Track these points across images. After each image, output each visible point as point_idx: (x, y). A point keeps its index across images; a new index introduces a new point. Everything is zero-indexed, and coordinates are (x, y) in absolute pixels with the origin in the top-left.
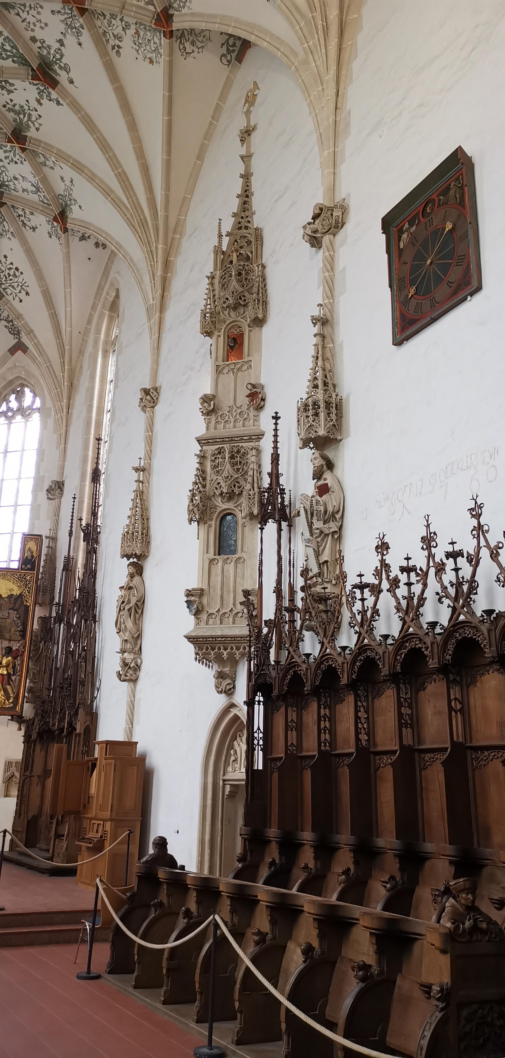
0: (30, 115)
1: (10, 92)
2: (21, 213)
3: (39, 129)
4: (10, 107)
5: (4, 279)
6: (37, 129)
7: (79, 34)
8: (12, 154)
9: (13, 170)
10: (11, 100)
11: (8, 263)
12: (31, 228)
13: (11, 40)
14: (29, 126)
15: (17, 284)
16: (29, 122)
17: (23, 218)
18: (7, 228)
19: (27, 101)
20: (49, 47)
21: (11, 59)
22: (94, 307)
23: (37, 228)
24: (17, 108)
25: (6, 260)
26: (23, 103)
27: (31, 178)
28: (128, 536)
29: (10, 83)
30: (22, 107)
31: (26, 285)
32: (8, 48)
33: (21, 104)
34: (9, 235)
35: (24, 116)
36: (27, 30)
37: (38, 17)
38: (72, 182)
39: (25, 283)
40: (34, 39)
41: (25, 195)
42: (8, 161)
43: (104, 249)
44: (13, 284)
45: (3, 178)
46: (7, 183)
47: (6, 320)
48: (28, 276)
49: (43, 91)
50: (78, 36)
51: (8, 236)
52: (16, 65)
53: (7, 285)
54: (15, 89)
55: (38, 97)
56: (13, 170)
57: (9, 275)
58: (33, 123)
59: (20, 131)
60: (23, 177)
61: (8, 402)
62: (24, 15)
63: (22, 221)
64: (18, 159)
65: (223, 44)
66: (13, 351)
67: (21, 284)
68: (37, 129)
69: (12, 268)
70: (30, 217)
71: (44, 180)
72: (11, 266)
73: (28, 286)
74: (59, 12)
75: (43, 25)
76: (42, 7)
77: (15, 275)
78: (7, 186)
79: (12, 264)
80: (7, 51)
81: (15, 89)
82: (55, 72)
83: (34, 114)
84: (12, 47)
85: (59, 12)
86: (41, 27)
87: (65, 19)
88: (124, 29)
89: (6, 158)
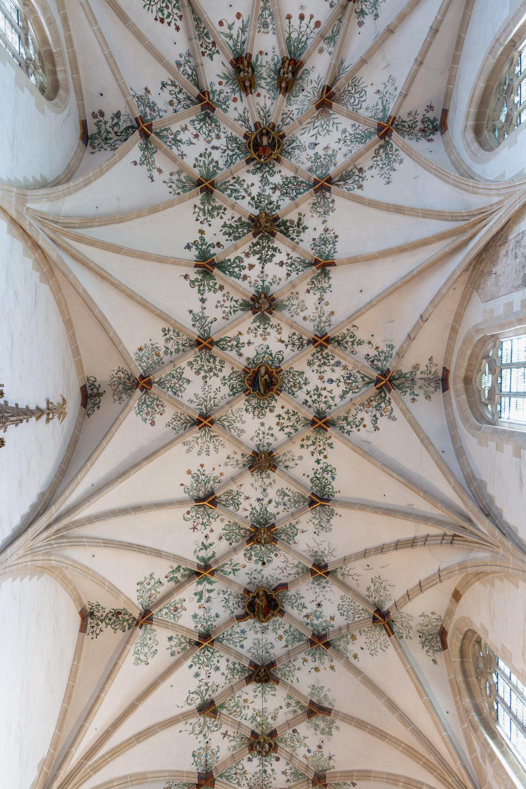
0: (204, 214)
1: (225, 225)
2: (181, 96)
3: (194, 208)
4: (221, 211)
6: (195, 206)
7: (194, 319)
8: (207, 162)
9: (201, 145)
10: (221, 218)
11: (172, 24)
13: (236, 277)
14: (202, 203)
16: (203, 207)
17: (177, 90)
18: (187, 68)
19: (210, 225)
20: (210, 290)
21: (232, 261)
22: (69, 40)
23: (161, 89)
24: (215, 213)
25: (175, 24)
26: (213, 221)
27: (184, 148)
29: (227, 234)
30: (212, 216)
32: (236, 270)
33: (213, 219)
34: (182, 60)
36: (228, 293)
37: (224, 309)
38: (152, 178)
39: (149, 8)
40: (221, 288)
41: (183, 123)
42: (208, 152)
43: (94, 113)
45: (206, 127)
46: (202, 124)
49: (202, 245)
50: (194, 317)
51: (183, 59)
52: (227, 258)
54: (221, 230)
55: (204, 236)
56: (201, 145)
57: (167, 7)
58: (200, 209)
59: (207, 193)
60: (191, 143)
62: (233, 303)
63: (176, 87)
65: (99, 386)
68: (195, 206)
69: (167, 18)
70: (170, 98)
71: (174, 159)
72: (169, 20)
73: (145, 6)
74: (212, 323)
75: (219, 305)
76: (224, 318)
77: (161, 10)
78: (201, 121)
79: (169, 24)
80: (236, 267)
81: (221, 230)
82: (198, 273)
84: (233, 272)
85: (212, 323)
86: (219, 302)
87: (206, 321)
88: (167, 348)
89: (210, 153)
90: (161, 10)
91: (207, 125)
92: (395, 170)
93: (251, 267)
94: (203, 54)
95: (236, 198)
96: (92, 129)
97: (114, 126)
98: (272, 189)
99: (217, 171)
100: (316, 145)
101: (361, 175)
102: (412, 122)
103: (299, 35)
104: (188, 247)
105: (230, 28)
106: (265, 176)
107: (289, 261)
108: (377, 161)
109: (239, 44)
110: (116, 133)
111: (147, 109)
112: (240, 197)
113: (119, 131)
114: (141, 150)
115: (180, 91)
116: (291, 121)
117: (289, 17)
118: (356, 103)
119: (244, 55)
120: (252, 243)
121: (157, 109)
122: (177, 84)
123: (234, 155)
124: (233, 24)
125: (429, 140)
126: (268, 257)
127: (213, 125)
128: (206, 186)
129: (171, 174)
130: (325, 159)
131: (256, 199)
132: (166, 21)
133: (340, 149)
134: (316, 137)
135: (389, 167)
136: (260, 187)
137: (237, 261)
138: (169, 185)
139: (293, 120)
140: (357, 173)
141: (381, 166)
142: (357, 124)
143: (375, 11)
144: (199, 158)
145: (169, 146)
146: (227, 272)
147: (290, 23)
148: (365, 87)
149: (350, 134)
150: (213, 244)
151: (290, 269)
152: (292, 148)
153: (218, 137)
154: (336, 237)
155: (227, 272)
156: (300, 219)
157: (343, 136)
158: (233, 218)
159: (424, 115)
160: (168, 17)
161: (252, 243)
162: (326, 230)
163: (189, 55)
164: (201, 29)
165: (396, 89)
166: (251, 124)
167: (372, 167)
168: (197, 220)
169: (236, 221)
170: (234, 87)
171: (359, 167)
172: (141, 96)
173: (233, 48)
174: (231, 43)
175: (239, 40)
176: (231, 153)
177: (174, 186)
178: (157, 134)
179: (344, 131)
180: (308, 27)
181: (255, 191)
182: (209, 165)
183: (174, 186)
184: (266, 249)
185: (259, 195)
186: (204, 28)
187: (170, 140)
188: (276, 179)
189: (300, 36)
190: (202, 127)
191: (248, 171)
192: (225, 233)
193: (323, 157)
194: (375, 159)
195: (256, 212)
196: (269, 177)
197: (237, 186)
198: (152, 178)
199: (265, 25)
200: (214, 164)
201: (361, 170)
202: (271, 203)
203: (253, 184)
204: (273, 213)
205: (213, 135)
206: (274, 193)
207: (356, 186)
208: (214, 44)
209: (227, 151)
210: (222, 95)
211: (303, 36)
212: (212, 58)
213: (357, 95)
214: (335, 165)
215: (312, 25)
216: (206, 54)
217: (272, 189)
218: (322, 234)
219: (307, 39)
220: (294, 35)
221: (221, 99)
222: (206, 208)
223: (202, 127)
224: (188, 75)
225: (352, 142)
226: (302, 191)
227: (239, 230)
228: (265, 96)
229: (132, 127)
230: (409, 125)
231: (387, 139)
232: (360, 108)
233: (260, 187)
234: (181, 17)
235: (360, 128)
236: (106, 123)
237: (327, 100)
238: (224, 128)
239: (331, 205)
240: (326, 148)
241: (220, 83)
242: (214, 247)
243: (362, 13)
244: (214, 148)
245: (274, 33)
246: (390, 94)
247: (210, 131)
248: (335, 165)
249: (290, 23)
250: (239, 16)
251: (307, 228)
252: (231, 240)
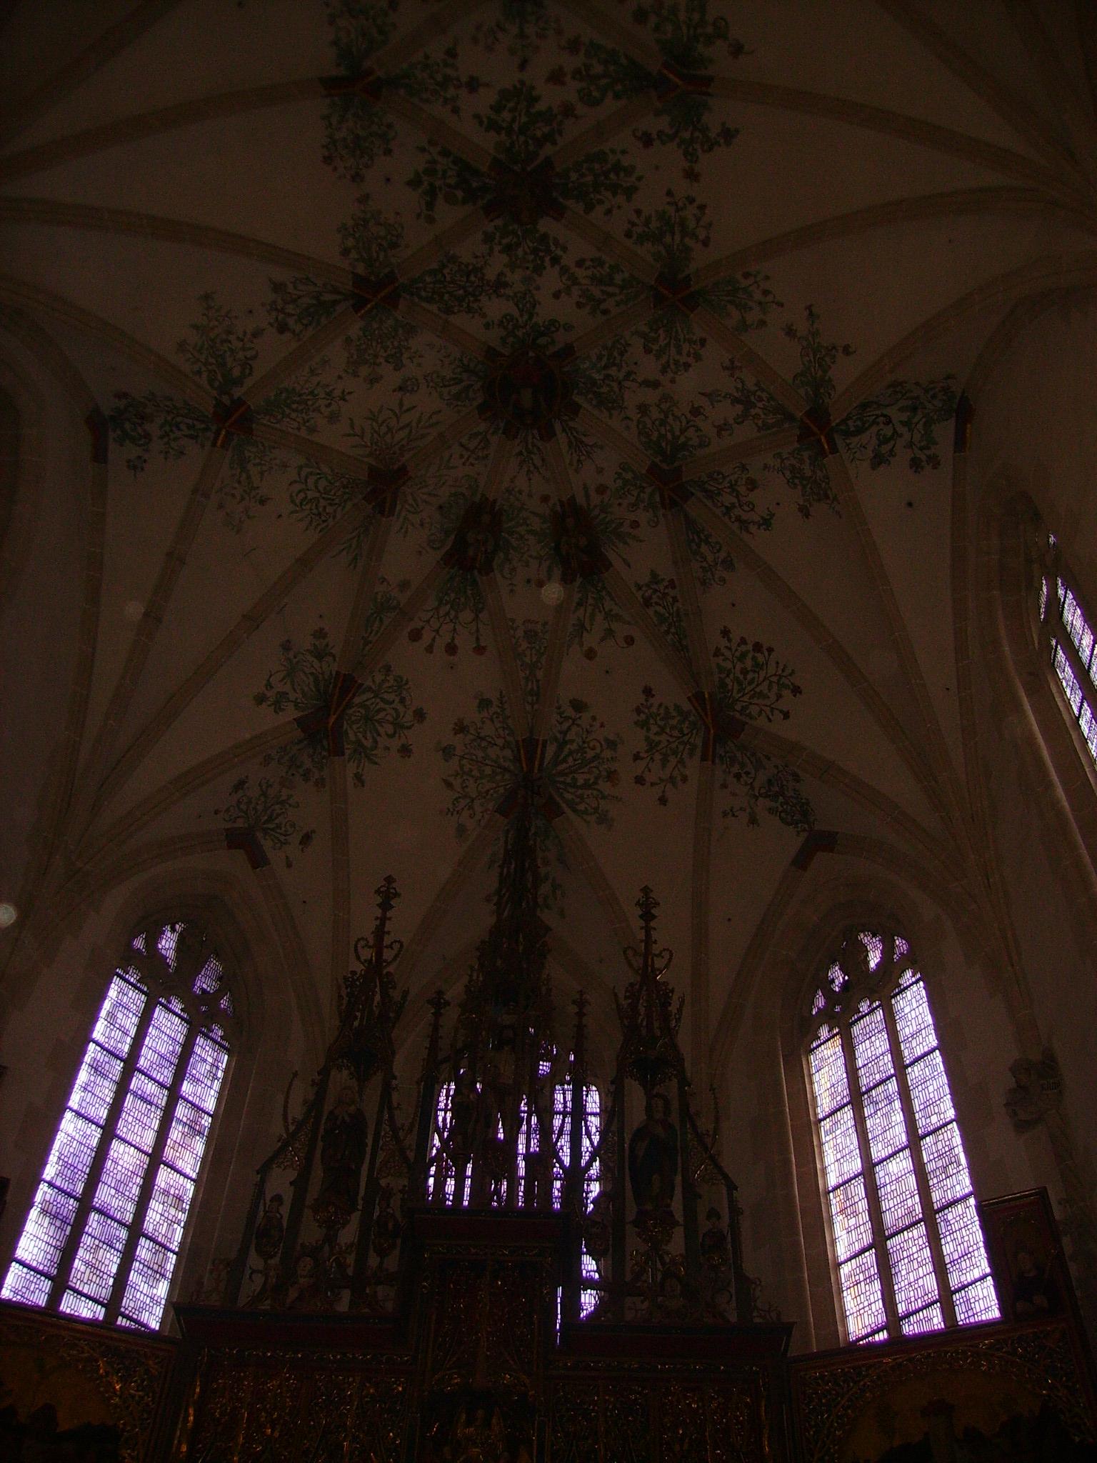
1: (630, 192)
2: (728, 499)
3: (708, 238)
4: (639, 230)
5: (736, 687)
6: (706, 243)
8: (673, 350)
12: (760, 526)
15: (766, 683)
16: (687, 240)
17: (737, 511)
18: (710, 558)
19: (669, 193)
21: (610, 95)
24: (654, 224)
25: (729, 640)
31: (788, 671)
32: (598, 69)
35: (673, 234)
38: (811, 314)
42: (670, 375)
44: (758, 690)
46: (682, 439)
47: (767, 796)
53: (746, 698)
54: (639, 179)
57: (744, 672)
63: (738, 519)
64: (688, 355)
66: (802, 861)
67: (774, 679)
69: (748, 652)
72: (744, 648)
77: (758, 666)
79: (743, 641)
89: (664, 371)
90: (758, 666)
91: (669, 436)
92: (195, 327)
93: (556, 77)
94: (672, 584)
95: (599, 262)
96: (945, 432)
97: (892, 438)
98: (506, 285)
99: (646, 330)
100: (400, 388)
101: (281, 317)
102: (172, 436)
103: (456, 617)
104: (728, 135)
105: (610, 633)
106: (526, 317)
107: (451, 92)
108: (243, 349)
109: (590, 601)
110: (889, 421)
111: (808, 473)
112: (588, 263)
113: (882, 426)
114: (830, 380)
115: (728, 509)
116: (464, 441)
117: (480, 650)
118: (311, 481)
119: (579, 580)
120: (554, 143)
121: (788, 474)
122: (735, 526)
123: (606, 367)
124: (602, 640)
125: (125, 395)
126: (511, 105)
127: (655, 436)
128: (676, 294)
129: (763, 323)
130: (376, 356)
131: (547, 259)
132: (750, 647)
133: (340, 377)
134: (401, 405)
135: (212, 335)
136: (538, 288)
137: (595, 94)
138: (770, 298)
139: (462, 445)
140: (291, 322)
141: (232, 337)
142: (303, 433)
143: (291, 655)
144: (691, 360)
145: (763, 390)
146: (624, 61)
147: (478, 639)
148: (296, 512)
149: (318, 410)
150: (663, 143)
151: (449, 71)
152: (461, 381)
153: (643, 409)
154: (328, 160)
155: (624, 61)
156: (430, 205)
157: (334, 407)
158: (609, 212)
159: (147, 451)
160: (743, 656)
161: (554, 143)
162: (357, 177)
163: (703, 583)
164: (673, 630)
165: (221, 506)
166: (562, 437)
167: (255, 335)
168: (702, 208)
169: (601, 202)
170: (603, 516)
171: (288, 335)
172: (819, 500)
173: (604, 593)
174: (608, 605)
175: (590, 609)
176: (613, 371)
177: (758, 296)
178: (791, 418)
179: (333, 418)
180: (437, 631)
181: (551, 279)
182: (669, 344)
183: (758, 296)
184: (516, 127)
185: (539, 270)
186: (667, 632)
187: (760, 405)
188: (496, 308)
189: (453, 613)
190: (682, 432)
191: (568, 328)
192: (629, 171)
193: (382, 360)
194: (249, 354)
195: (546, 225)
196: (516, 313)
197: (596, 292)
198: (811, 314)
200: (655, 347)
201: (283, 328)
202: (508, 249)
203: (556, 295)
204: (499, 222)
205: (655, 414)
206: (501, 274)
207: (290, 288)
208: (647, 602)
209: (621, 375)
210: (632, 499)
211: (448, 614)
212: (654, 575)
213: (310, 495)
214: (348, 341)
215: (427, 637)
216: (666, 583)
217: (506, 285)
218: (367, 166)
219: (437, 609)
220: (467, 615)
221: (635, 493)
222: (677, 237)
223: (682, 432)
224: (707, 543)
225: (312, 393)
226: (428, 279)
227: (589, 178)
228: (530, 495)
229: (848, 434)
230: (179, 429)
231: (226, 400)
232: (301, 467)
233: (538, 288)
234: (717, 653)
235: (296, 425)
236: (910, 445)
237: (383, 485)
238: (628, 428)
239: (350, 242)
240: (373, 380)
241: (635, 524)
242: (660, 133)
244: (656, 385)
245: (513, 621)
246: (233, 495)
247: (663, 423)
248: (348, 341)
249: (478, 639)
250: (590, 654)
251: (409, 183)
252: (613, 151)
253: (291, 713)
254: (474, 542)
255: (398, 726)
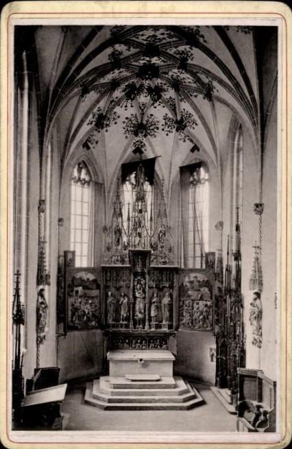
28: (253, 281)
41: (190, 84)
48: (195, 117)
61: (193, 176)
66: (193, 150)
83: (189, 53)
93: (163, 34)
199: (143, 105)
243: (99, 111)
253: (94, 123)
254: (132, 92)
255: (114, 119)
